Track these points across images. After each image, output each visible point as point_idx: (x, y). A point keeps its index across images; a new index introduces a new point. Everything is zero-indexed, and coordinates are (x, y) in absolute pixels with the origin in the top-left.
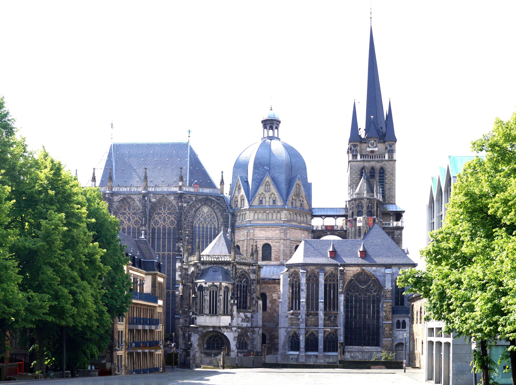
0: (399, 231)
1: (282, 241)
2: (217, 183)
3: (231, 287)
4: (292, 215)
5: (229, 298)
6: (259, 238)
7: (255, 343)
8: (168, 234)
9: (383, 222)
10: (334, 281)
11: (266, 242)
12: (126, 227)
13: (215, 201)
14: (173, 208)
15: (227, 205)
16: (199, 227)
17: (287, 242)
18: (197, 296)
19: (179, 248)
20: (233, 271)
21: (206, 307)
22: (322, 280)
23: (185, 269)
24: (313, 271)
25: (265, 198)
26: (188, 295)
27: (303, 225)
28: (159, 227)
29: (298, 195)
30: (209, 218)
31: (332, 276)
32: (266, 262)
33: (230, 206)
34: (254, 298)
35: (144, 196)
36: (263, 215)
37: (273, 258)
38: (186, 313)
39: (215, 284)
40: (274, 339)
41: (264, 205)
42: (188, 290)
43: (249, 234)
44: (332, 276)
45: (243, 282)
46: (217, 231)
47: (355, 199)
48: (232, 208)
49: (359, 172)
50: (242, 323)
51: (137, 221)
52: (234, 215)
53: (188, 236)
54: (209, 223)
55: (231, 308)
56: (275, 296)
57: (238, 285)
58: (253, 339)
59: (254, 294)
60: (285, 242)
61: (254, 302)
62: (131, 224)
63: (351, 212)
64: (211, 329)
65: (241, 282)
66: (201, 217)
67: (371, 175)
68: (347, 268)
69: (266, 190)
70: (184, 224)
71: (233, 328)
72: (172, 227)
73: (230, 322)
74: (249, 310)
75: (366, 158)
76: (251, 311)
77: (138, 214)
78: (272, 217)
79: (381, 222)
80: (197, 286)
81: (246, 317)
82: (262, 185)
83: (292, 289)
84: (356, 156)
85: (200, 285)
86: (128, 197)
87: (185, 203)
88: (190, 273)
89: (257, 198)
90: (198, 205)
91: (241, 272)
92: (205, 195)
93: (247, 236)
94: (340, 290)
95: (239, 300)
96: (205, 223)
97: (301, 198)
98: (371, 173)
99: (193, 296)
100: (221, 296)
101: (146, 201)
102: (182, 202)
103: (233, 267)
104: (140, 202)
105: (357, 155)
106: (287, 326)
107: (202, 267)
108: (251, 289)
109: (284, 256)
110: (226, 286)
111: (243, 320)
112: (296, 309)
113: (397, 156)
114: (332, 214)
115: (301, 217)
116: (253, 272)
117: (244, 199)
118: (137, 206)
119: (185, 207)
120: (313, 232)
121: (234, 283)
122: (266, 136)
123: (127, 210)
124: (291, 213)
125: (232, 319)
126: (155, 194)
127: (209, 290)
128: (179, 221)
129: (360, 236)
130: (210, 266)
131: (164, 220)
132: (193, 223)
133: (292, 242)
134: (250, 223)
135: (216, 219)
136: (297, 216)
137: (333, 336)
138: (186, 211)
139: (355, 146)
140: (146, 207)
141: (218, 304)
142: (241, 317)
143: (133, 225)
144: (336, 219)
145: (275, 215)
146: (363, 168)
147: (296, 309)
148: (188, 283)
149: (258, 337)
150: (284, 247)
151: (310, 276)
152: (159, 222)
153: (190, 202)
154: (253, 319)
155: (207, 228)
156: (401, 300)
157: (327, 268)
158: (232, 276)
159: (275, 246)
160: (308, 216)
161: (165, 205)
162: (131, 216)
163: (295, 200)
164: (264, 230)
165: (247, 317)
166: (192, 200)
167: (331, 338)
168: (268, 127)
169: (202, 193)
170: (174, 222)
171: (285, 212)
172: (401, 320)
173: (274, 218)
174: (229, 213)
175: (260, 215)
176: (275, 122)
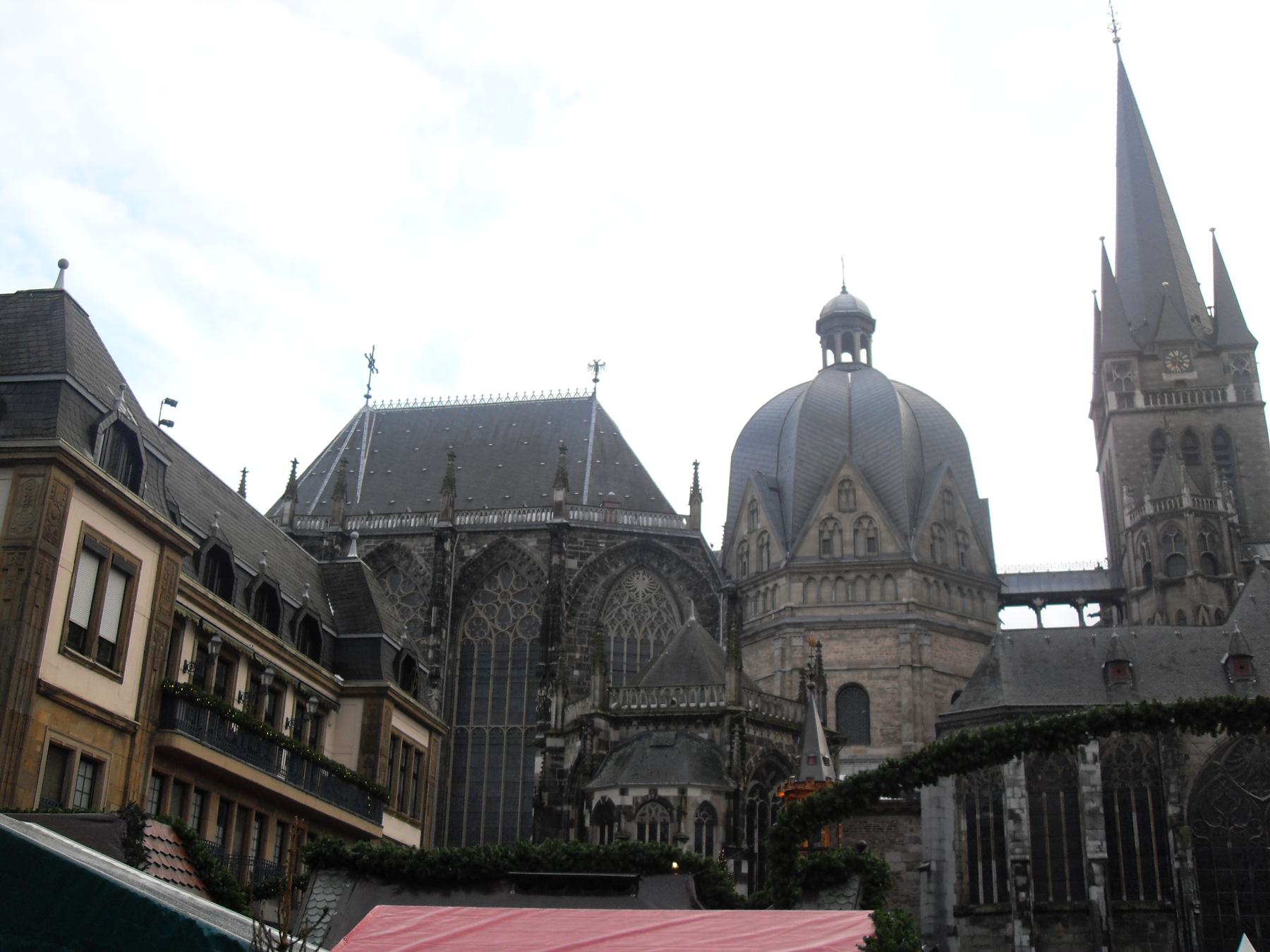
1: (906, 673)
2: (681, 506)
3: (721, 805)
4: (934, 588)
8: (514, 662)
11: (847, 678)
13: (671, 553)
14: (532, 579)
15: (711, 568)
16: (619, 640)
17: (922, 676)
20: (731, 744)
25: (841, 531)
27: (973, 624)
28: (485, 641)
29: (947, 523)
30: (653, 610)
32: (853, 748)
33: (724, 570)
35: (440, 536)
36: (834, 587)
37: (875, 734)
39: (662, 792)
41: (837, 554)
43: (788, 651)
47: (1151, 517)
48: (729, 577)
49: (1146, 446)
52: (735, 598)
53: (579, 667)
54: (652, 626)
60: (917, 678)
65: (763, 795)
66: (627, 607)
69: (843, 507)
70: (569, 628)
75: (1162, 402)
77: (421, 598)
78: (868, 594)
80: (589, 806)
82: (829, 490)
85: (603, 798)
86: (392, 546)
87: (570, 557)
88: (568, 764)
89: (814, 532)
90: (616, 566)
92: (639, 535)
93: (783, 660)
94: (1172, 810)
95: (756, 867)
96: (639, 624)
97: (960, 536)
98: (1184, 449)
100: (684, 840)
101: (445, 554)
102: (560, 552)
103: (732, 726)
104: (427, 561)
105: (1134, 394)
107: (614, 735)
114: (1065, 588)
115: (963, 595)
117: (768, 544)
119: (572, 571)
121: (737, 790)
124: (932, 579)
126: (474, 534)
127: (638, 818)
130: (643, 729)
131: (503, 618)
133: (940, 677)
134: (793, 616)
135: (677, 615)
136: (950, 592)
138: (576, 585)
139: (1123, 368)
140: (444, 571)
144: (1079, 610)
145: (876, 585)
148: (560, 804)
150: (915, 695)
152: (485, 625)
153: (588, 555)
155: (645, 643)
158: (727, 764)
159: (882, 691)
160: (986, 595)
161: (507, 566)
163: (941, 540)
164: (841, 637)
166: (597, 548)
168: (838, 338)
169: (632, 526)
171: (910, 573)
173: (875, 596)
174: (718, 592)
175: (826, 590)
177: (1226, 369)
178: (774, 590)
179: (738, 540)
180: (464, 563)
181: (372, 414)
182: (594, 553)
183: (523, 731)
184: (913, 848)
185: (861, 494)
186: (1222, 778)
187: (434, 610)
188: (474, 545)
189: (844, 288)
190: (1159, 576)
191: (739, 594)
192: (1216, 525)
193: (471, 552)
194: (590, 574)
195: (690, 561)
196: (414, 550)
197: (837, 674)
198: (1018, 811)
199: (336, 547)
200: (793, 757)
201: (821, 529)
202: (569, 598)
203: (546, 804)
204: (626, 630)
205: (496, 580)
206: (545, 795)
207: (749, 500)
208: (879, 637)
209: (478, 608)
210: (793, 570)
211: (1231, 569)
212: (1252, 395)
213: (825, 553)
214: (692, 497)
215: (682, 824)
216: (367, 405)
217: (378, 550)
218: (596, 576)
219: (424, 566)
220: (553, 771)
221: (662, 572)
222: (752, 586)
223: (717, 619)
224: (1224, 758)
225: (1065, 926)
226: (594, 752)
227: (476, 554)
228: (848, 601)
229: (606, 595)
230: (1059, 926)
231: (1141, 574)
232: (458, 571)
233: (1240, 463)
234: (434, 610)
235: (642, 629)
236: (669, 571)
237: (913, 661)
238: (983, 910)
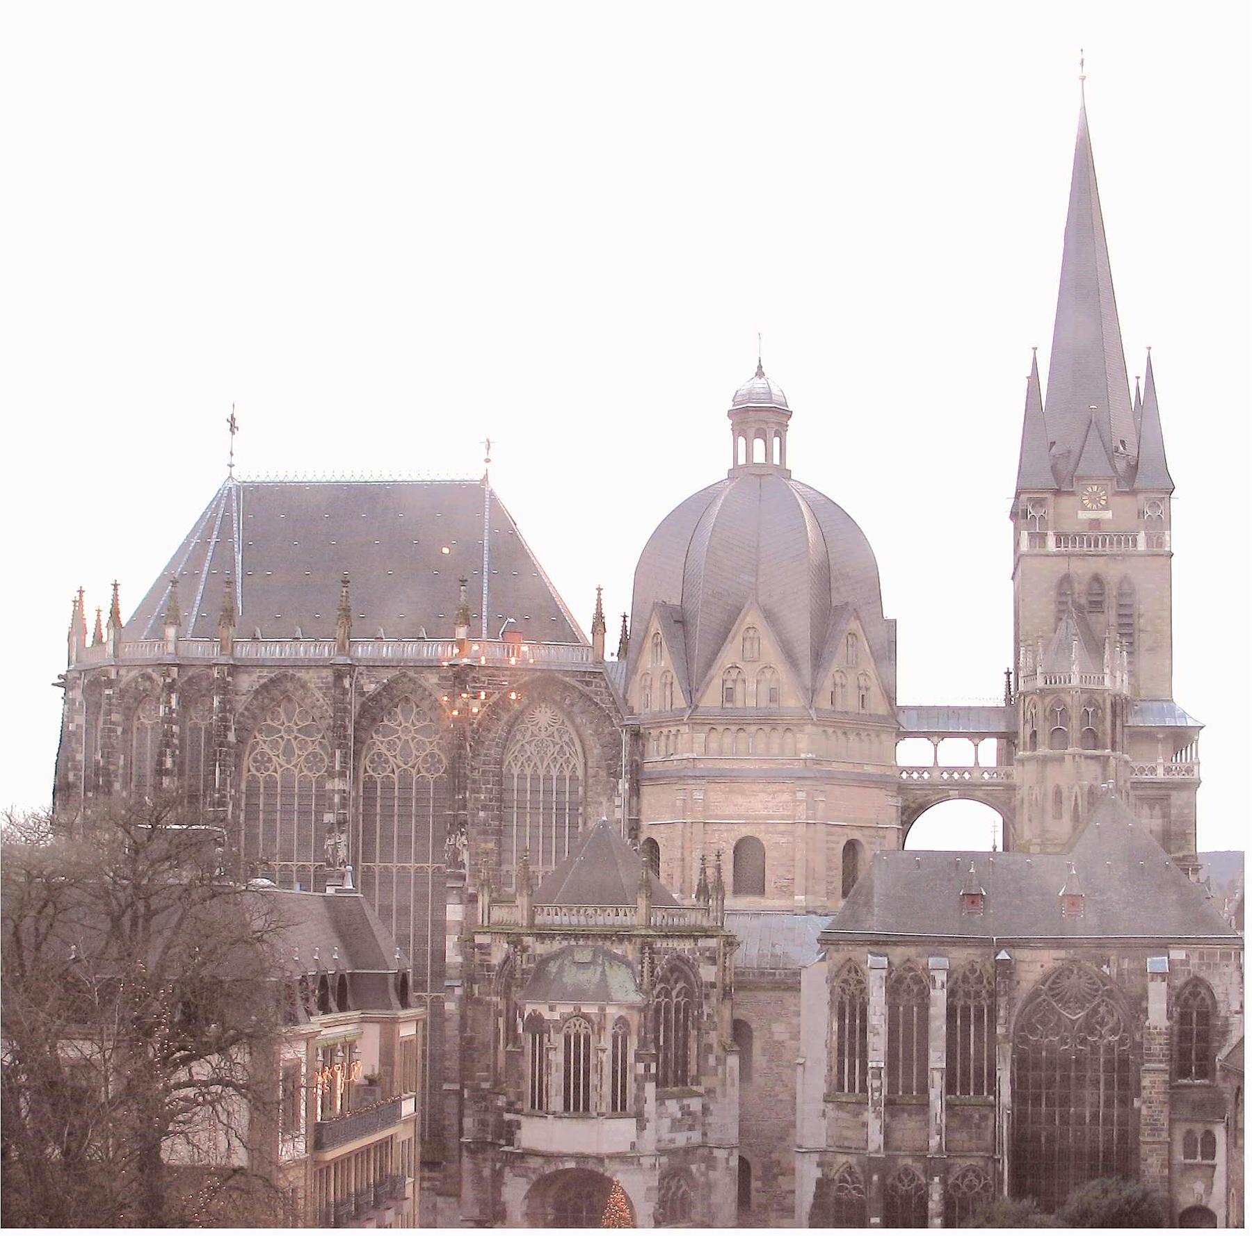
0: (1184, 795)
1: (801, 830)
3: (635, 1019)
5: (631, 1058)
6: (726, 817)
7: (716, 1198)
9: (1133, 764)
10: (978, 994)
12: (278, 776)
15: (614, 702)
16: (522, 777)
18: (523, 1047)
19: (456, 853)
21: (552, 1092)
22: (939, 997)
23: (480, 946)
24: (908, 960)
25: (744, 681)
26: (490, 1037)
27: (868, 769)
30: (555, 744)
31: (972, 978)
32: (748, 899)
33: (626, 701)
34: (709, 1048)
37: (769, 886)
38: (484, 1098)
39: (584, 1010)
40: (775, 1177)
41: (739, 704)
42: (492, 1019)
44: (972, 978)
45: (674, 993)
46: (580, 788)
49: (1052, 593)
50: (673, 1135)
51: (315, 755)
52: (637, 735)
53: (484, 808)
55: (638, 1089)
56: (780, 1030)
57: (657, 1010)
58: (710, 1186)
59: (713, 1034)
61: (712, 1060)
62: (295, 766)
63: (1029, 731)
64: (571, 1165)
65: (668, 994)
67: (1090, 602)
68: (1021, 954)
69: (747, 654)
70: (473, 769)
71: (642, 1160)
72: (430, 778)
73: (634, 1140)
74: (695, 1088)
76: (701, 1089)
79: (1126, 762)
80: (522, 1017)
81: (686, 1111)
83: (841, 1018)
84: (1043, 537)
89: (717, 682)
91: (668, 961)
94: (1000, 1030)
97: (862, 678)
99: (509, 1048)
100: (604, 1051)
101: (345, 692)
103: (642, 948)
104: (325, 694)
106: (823, 1145)
107: (540, 948)
108: (701, 1015)
109: (807, 880)
110: (621, 1018)
111: (676, 1125)
112: (852, 1088)
113: (1180, 538)
115: (861, 740)
116: (709, 958)
117: (672, 683)
118: (315, 706)
120: (902, 788)
122: (742, 460)
123: (283, 717)
125: (641, 1127)
128: (457, 760)
129: (1058, 816)
130: (565, 943)
131: (406, 755)
132: (500, 763)
135: (579, 750)
137: (976, 1182)
138: (480, 724)
140: (345, 710)
141: (594, 1079)
142: (670, 1116)
143: (301, 771)
146: (1066, 579)
147: (852, 1088)
149: (728, 1179)
151: (899, 980)
152: (387, 761)
154: (710, 1119)
155: (548, 778)
156: (1197, 1060)
157: (961, 956)
161: (407, 699)
162: (296, 738)
163: (843, 686)
165: (690, 1114)
167: (971, 1188)
168: (751, 432)
170: (440, 761)
171: (809, 729)
172: (1199, 1129)
173: (775, 749)
174: (620, 727)
175: (728, 739)
176: (772, 417)
177: (1141, 513)
178: (676, 735)
179: (640, 672)
180: (364, 699)
181: (238, 488)
182: (497, 692)
183: (430, 871)
184: (794, 1021)
185: (764, 642)
186: (1044, 1000)
187: (338, 752)
188: (373, 679)
189: (760, 367)
190: (1042, 750)
191: (642, 731)
192: (1101, 701)
193: (371, 688)
194: (494, 712)
195: (593, 696)
196: (310, 682)
197: (736, 826)
198: (877, 1026)
199: (229, 679)
200: (694, 959)
201: (725, 677)
202: (473, 738)
203: (477, 995)
204: (529, 766)
205: (396, 713)
206: (476, 987)
207: (653, 631)
208: (774, 793)
209: (379, 742)
210: (695, 717)
211: (1109, 745)
212: (1161, 543)
213: (727, 701)
214: (594, 626)
215: (602, 1037)
216: (230, 477)
217: (272, 680)
218: (498, 713)
219: (321, 699)
220: (482, 965)
221: (565, 706)
222: (654, 725)
223: (619, 753)
224: (1047, 985)
225: (910, 1115)
226: (524, 967)
227: (376, 690)
228: (749, 754)
229: (509, 732)
230: (906, 1115)
231: (1028, 739)
232: (357, 707)
233: (1140, 616)
234: (338, 752)
235: (545, 764)
236: (572, 705)
237: (807, 819)
238: (844, 1099)
